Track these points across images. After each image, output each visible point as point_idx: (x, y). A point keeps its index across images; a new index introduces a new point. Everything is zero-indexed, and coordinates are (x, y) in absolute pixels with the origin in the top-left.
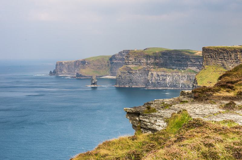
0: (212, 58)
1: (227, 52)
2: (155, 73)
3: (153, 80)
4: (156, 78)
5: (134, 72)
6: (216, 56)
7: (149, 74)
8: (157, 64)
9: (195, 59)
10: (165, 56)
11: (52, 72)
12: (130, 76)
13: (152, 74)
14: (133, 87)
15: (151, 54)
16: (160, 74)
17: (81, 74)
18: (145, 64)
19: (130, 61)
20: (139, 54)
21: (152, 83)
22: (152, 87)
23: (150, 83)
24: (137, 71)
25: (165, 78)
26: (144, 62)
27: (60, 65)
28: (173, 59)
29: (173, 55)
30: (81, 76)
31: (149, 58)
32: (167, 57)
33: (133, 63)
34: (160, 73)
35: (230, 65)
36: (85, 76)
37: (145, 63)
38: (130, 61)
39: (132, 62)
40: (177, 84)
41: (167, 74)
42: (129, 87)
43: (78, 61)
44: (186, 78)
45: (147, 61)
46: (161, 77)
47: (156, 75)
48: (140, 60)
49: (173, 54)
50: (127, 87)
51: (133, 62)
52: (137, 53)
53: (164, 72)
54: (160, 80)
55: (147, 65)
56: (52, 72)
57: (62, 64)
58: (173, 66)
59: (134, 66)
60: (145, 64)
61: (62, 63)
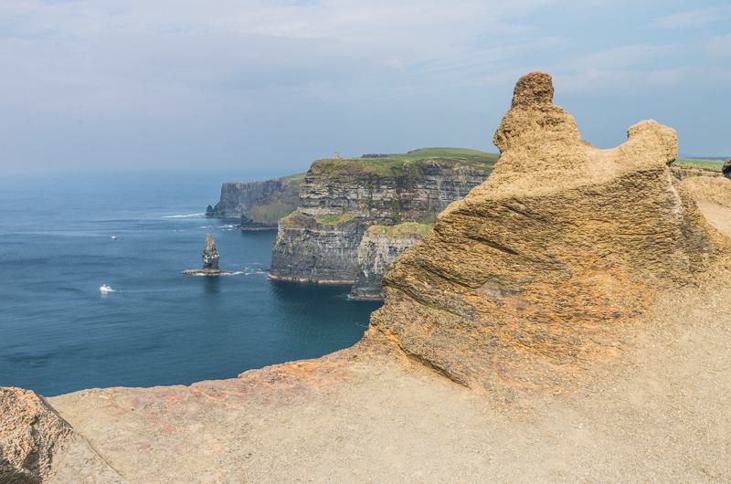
2: (383, 244)
3: (376, 264)
4: (387, 257)
5: (323, 232)
7: (362, 243)
8: (405, 206)
10: (433, 178)
11: (213, 207)
13: (372, 245)
14: (320, 282)
15: (382, 170)
16: (399, 244)
17: (252, 218)
18: (361, 206)
19: (312, 196)
20: (345, 172)
21: (373, 276)
22: (370, 292)
23: (367, 275)
24: (333, 229)
26: (360, 198)
27: (229, 191)
28: (457, 189)
29: (458, 174)
30: (251, 223)
31: (378, 183)
32: (439, 180)
33: (322, 202)
36: (261, 225)
37: (362, 201)
38: (312, 196)
39: (319, 196)
42: (310, 281)
43: (271, 181)
47: (388, 250)
48: (345, 192)
49: (457, 172)
50: (302, 280)
52: (339, 167)
53: (415, 238)
55: (371, 207)
56: (213, 207)
57: (236, 190)
59: (327, 211)
60: (361, 206)
61: (234, 185)
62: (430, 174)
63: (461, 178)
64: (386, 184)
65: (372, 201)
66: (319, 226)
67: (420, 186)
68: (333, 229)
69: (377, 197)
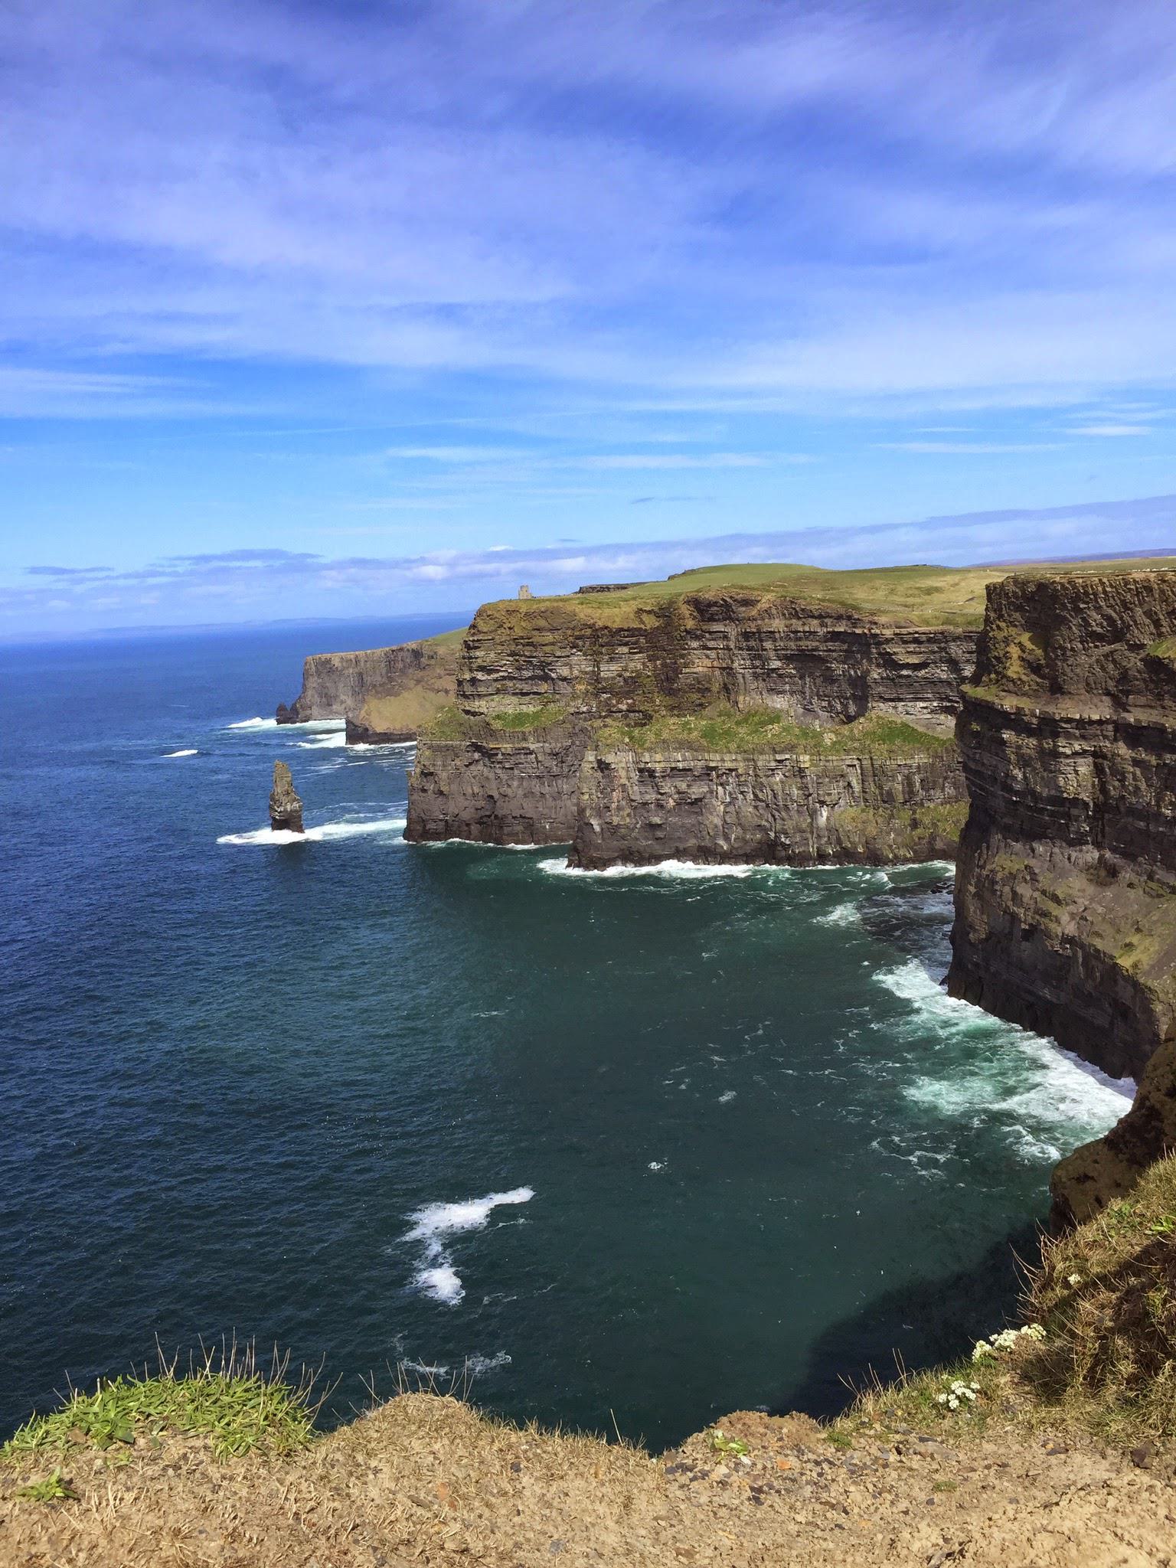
2: (621, 761)
9: (916, 641)
13: (603, 766)
16: (657, 761)
19: (480, 676)
20: (542, 623)
23: (597, 828)
25: (697, 790)
26: (576, 673)
28: (768, 645)
32: (732, 630)
34: (658, 757)
38: (480, 676)
39: (495, 676)
40: (786, 833)
41: (714, 760)
44: (857, 788)
45: (597, 664)
46: (667, 787)
47: (635, 776)
51: (504, 678)
54: (662, 806)
58: (771, 690)
62: (712, 619)
63: (778, 624)
64: (626, 644)
65: (598, 681)
66: (493, 734)
67: (695, 644)
68: (525, 739)
69: (609, 670)
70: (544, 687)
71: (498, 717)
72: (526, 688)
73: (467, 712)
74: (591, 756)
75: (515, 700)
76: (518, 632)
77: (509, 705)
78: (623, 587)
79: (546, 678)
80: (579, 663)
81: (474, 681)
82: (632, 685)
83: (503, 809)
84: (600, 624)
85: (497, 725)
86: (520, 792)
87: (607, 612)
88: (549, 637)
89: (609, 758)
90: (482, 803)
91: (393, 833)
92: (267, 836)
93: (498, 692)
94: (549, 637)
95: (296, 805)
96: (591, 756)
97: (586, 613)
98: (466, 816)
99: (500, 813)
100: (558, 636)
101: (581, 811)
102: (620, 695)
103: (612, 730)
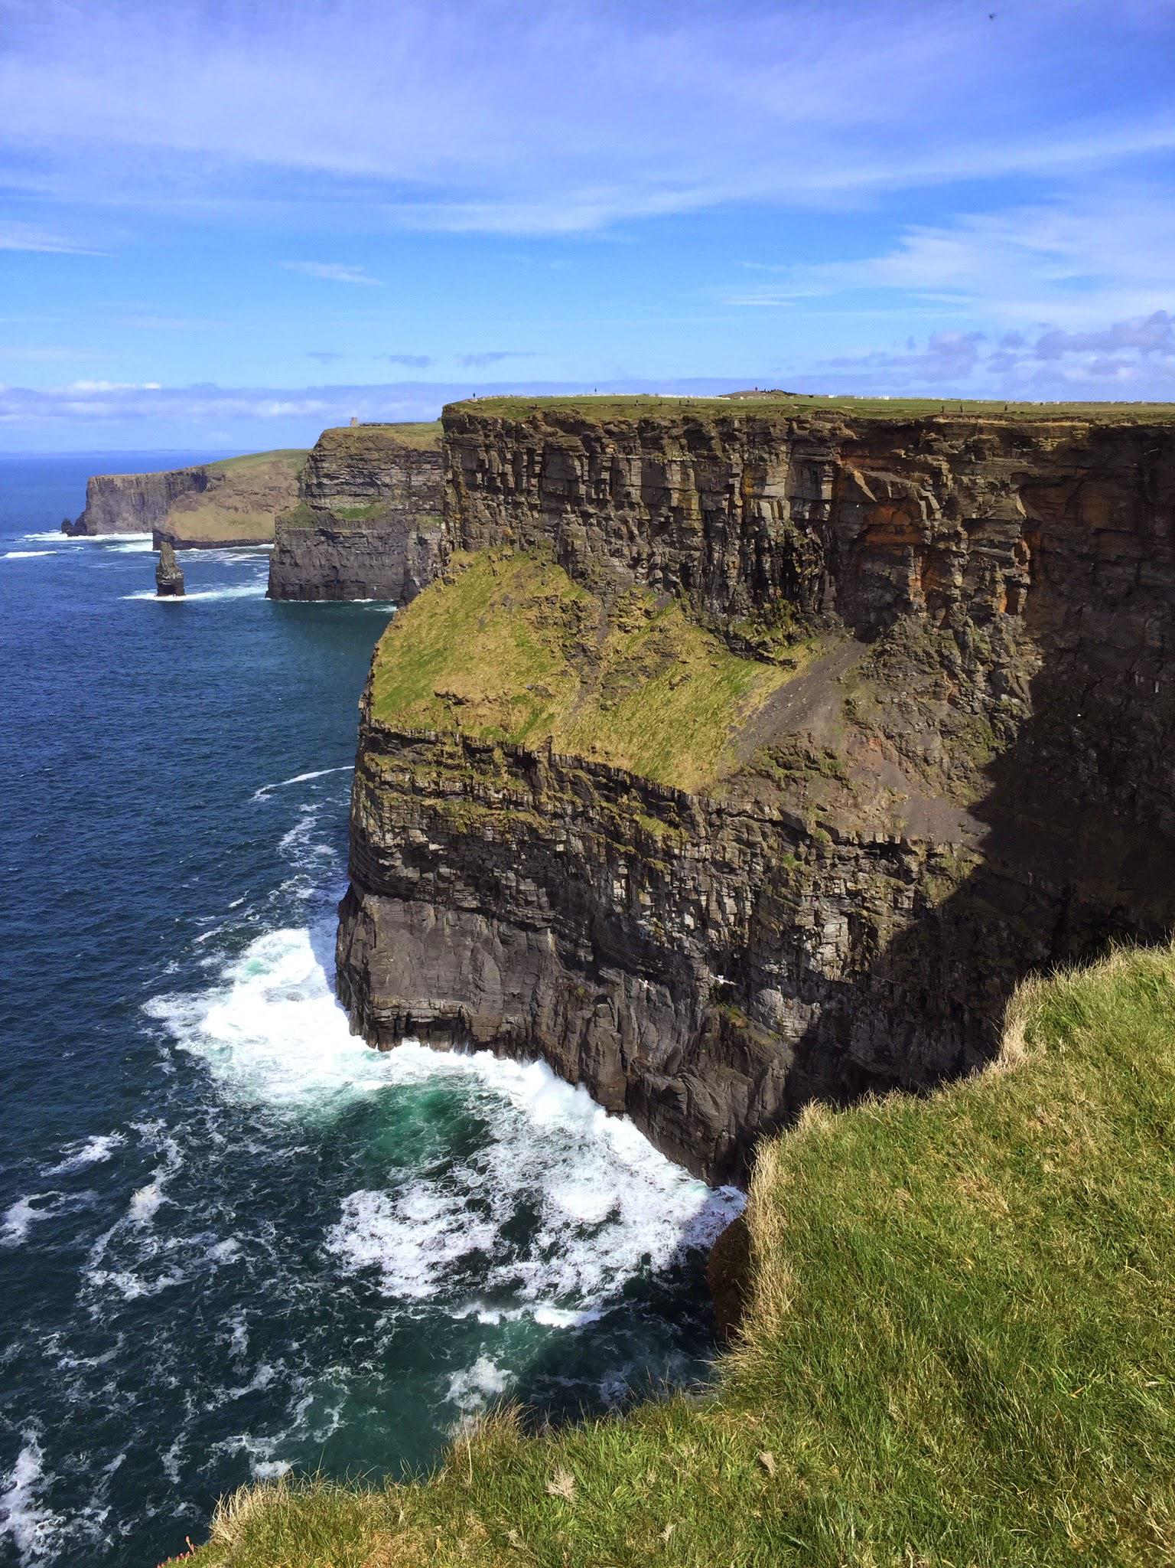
0: (496, 491)
1: (587, 442)
6: (517, 475)
12: (330, 549)
13: (422, 541)
19: (325, 481)
35: (617, 553)
38: (325, 481)
45: (409, 476)
65: (410, 487)
66: (335, 522)
69: (417, 480)
70: (371, 491)
71: (339, 511)
72: (359, 491)
73: (314, 507)
74: (414, 535)
75: (350, 499)
76: (353, 451)
77: (346, 503)
78: (412, 424)
79: (373, 484)
80: (395, 475)
81: (320, 485)
82: (434, 491)
83: (344, 575)
84: (411, 447)
85: (339, 516)
86: (356, 564)
87: (416, 439)
88: (376, 455)
89: (427, 536)
90: (326, 572)
91: (260, 595)
92: (151, 596)
93: (338, 493)
94: (376, 455)
95: (179, 574)
96: (414, 535)
97: (400, 439)
98: (315, 581)
99: (342, 578)
100: (382, 454)
101: (407, 572)
102: (425, 498)
103: (426, 520)
